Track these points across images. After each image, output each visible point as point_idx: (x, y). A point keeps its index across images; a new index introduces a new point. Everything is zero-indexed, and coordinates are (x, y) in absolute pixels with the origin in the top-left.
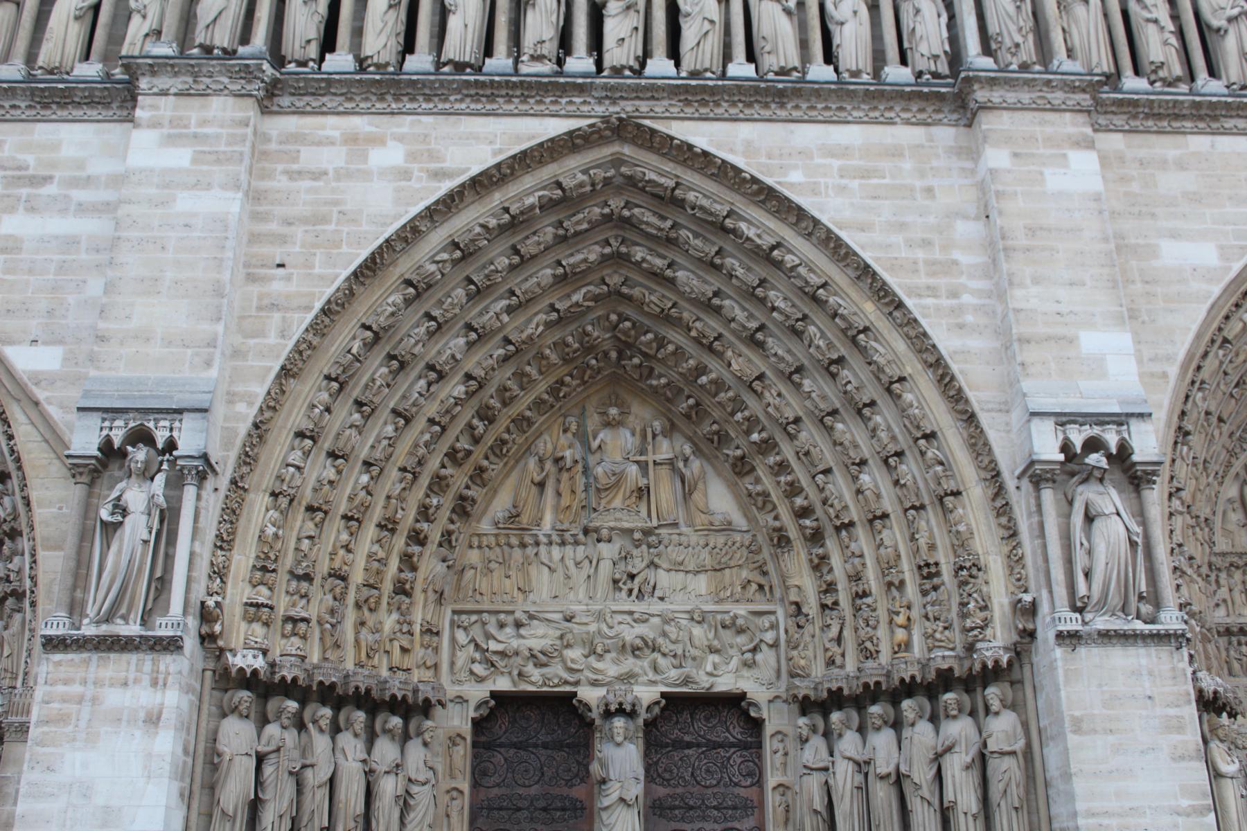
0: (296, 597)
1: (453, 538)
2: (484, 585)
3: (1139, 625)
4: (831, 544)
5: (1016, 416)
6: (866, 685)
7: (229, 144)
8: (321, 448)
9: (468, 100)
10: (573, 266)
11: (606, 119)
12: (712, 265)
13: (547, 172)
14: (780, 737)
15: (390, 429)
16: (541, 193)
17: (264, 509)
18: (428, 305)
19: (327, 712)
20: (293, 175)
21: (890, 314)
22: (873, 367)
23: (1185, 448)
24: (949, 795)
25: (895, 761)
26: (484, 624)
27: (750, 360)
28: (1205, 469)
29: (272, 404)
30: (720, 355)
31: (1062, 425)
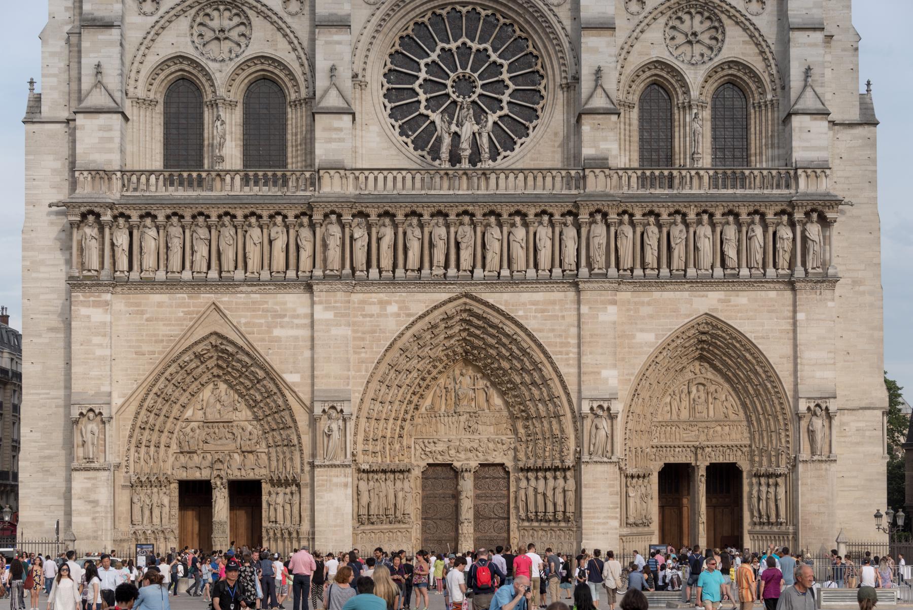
3: (605, 459)
20: (364, 316)
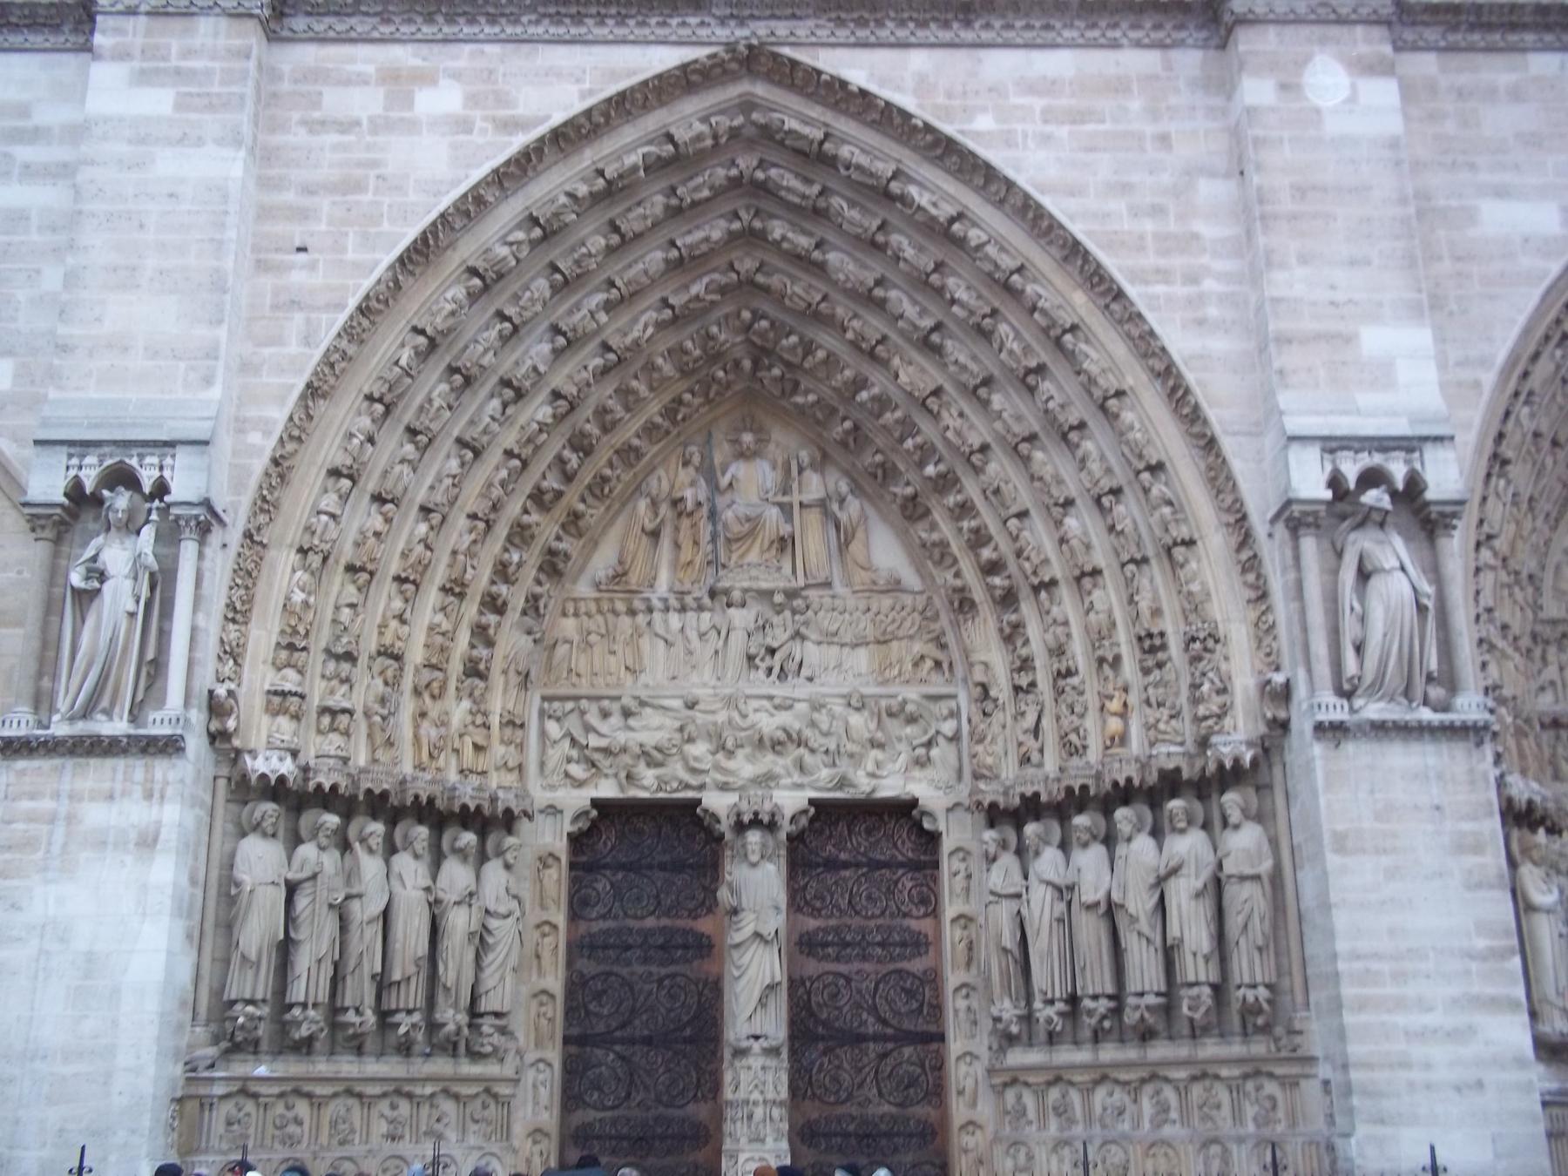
0: (335, 682)
1: (541, 605)
2: (582, 663)
3: (1426, 714)
4: (1027, 609)
5: (1270, 441)
6: (1069, 790)
7: (223, 83)
8: (365, 490)
9: (546, 21)
10: (691, 247)
11: (731, 47)
12: (874, 244)
13: (652, 122)
14: (961, 855)
15: (453, 465)
16: (646, 149)
17: (289, 569)
18: (500, 300)
19: (378, 828)
20: (316, 126)
21: (1107, 306)
22: (1083, 378)
23: (1502, 483)
24: (1174, 930)
25: (1106, 886)
26: (583, 713)
27: (923, 370)
28: (1531, 508)
29: (297, 433)
30: (884, 363)
31: (1332, 451)
